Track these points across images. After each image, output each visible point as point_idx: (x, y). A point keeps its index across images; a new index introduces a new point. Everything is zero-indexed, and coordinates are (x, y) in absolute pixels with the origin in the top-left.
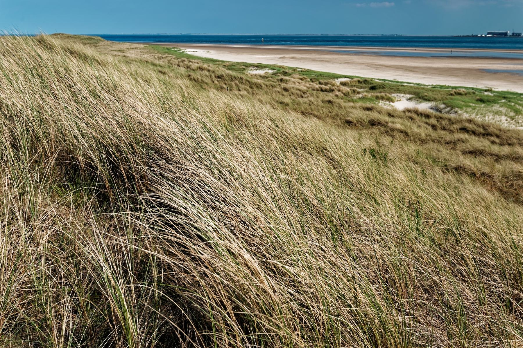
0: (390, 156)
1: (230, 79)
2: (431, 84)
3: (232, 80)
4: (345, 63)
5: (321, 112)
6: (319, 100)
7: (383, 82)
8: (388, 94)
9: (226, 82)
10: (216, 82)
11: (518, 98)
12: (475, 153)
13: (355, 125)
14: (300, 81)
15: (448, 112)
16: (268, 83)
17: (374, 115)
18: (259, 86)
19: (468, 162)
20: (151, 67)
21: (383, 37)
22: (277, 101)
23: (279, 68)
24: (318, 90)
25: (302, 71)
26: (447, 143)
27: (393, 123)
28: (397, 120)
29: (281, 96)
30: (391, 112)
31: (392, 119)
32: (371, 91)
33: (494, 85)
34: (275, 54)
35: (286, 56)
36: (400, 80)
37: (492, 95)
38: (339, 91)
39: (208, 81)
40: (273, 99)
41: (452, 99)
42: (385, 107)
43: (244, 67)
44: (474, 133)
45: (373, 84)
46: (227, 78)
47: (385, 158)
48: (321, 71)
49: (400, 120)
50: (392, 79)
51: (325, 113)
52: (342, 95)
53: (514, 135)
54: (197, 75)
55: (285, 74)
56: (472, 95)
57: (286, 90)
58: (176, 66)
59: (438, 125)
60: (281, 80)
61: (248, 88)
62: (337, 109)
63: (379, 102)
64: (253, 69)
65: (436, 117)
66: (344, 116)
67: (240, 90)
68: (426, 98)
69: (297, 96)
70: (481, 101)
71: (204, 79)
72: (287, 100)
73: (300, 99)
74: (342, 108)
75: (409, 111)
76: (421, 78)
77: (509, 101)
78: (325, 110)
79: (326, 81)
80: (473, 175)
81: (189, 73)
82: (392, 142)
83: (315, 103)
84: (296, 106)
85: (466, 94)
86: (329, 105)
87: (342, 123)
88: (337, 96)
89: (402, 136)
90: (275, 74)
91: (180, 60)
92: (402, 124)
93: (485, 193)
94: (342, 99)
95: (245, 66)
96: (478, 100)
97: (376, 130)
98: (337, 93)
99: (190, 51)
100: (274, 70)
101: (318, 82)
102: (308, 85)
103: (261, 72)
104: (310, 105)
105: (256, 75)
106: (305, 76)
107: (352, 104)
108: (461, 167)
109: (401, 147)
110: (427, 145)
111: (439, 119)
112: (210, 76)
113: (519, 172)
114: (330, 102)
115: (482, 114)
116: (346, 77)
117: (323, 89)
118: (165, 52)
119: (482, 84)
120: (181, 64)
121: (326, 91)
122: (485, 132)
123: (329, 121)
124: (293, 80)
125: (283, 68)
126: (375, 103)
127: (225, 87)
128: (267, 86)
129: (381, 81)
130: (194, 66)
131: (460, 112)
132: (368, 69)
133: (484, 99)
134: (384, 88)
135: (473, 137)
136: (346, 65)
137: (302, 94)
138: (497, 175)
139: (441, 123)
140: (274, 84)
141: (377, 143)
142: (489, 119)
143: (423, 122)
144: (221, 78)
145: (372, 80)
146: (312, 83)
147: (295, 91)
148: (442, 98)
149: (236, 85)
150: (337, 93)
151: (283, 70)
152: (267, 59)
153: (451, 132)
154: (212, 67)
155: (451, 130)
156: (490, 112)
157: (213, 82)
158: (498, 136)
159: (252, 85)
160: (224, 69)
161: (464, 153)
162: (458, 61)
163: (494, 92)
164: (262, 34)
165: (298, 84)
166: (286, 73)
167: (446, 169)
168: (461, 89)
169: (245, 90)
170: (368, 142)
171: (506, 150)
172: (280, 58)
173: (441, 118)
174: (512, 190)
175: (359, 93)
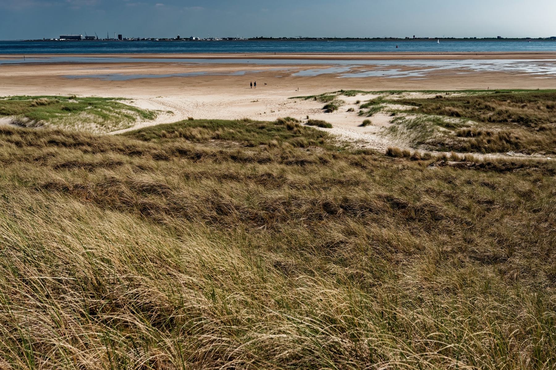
2: (7, 96)
11: (104, 103)
12: (67, 165)
15: (33, 125)
19: (59, 177)
26: (37, 160)
33: (78, 92)
37: (77, 102)
41: (34, 111)
44: (65, 144)
53: (105, 141)
56: (56, 104)
65: (18, 132)
68: (4, 112)
70: (67, 109)
77: (96, 107)
80: (65, 190)
85: (49, 104)
96: (63, 109)
108: (51, 184)
110: (13, 166)
111: (22, 134)
113: (113, 178)
115: (70, 124)
119: (65, 92)
122: (76, 142)
131: (46, 124)
133: (70, 108)
135: (64, 149)
139: (25, 139)
143: (3, 140)
148: (23, 110)
153: (39, 147)
155: (38, 145)
156: (78, 120)
158: (89, 145)
161: (56, 168)
163: (79, 99)
167: (35, 188)
168: (43, 99)
171: (99, 157)
173: (24, 133)
174: (107, 197)
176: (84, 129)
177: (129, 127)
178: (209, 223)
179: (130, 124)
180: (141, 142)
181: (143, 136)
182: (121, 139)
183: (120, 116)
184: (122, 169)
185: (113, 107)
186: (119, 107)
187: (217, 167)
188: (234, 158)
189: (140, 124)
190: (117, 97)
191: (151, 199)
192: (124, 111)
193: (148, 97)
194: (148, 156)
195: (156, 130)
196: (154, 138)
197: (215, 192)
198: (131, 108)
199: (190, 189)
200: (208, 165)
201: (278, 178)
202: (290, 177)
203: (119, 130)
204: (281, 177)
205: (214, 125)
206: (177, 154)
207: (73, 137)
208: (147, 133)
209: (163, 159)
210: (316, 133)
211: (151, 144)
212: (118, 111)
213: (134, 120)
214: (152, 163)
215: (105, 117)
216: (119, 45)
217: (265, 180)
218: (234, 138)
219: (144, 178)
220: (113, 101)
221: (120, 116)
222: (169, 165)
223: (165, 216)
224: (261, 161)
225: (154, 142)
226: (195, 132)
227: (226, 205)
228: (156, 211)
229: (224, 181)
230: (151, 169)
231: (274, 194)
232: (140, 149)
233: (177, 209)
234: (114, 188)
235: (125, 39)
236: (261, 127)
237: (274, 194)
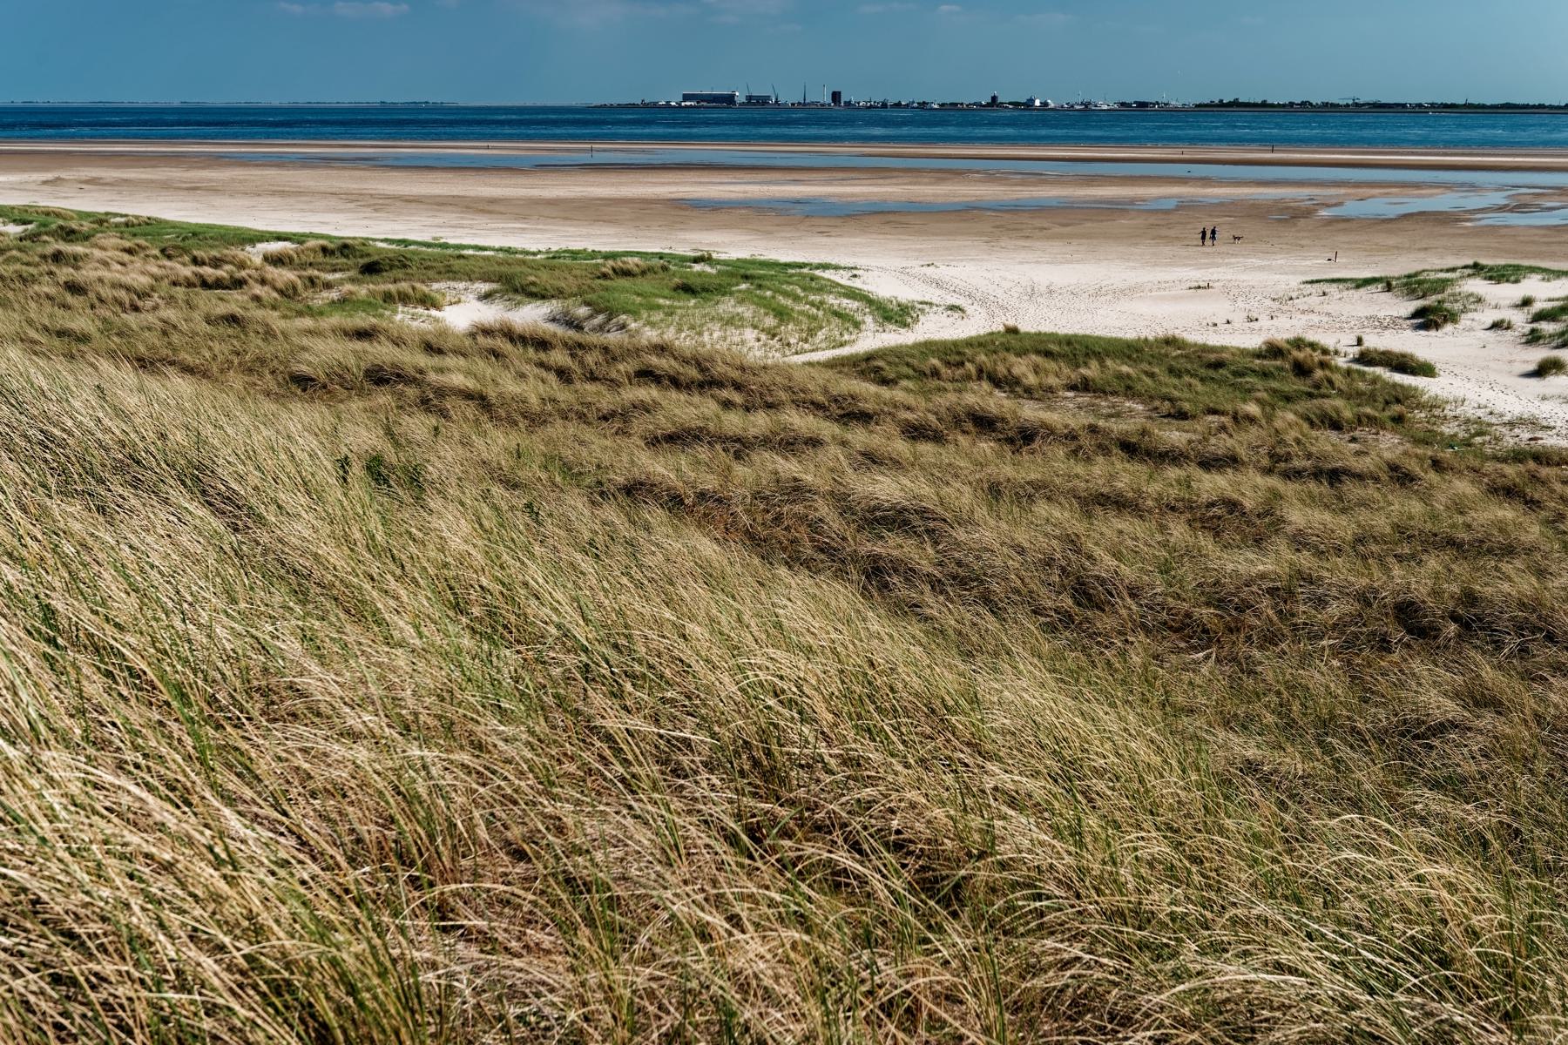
0: (432, 472)
4: (273, 193)
5: (207, 355)
6: (197, 316)
7: (401, 248)
8: (418, 285)
11: (782, 277)
12: (678, 438)
13: (325, 387)
14: (126, 257)
15: (601, 328)
17: (382, 352)
19: (660, 467)
21: (385, 108)
22: (46, 329)
23: (42, 218)
24: (190, 284)
25: (127, 225)
26: (605, 418)
27: (441, 371)
28: (450, 361)
29: (60, 312)
30: (433, 341)
31: (436, 361)
32: (367, 277)
33: (717, 244)
34: (24, 170)
36: (452, 241)
37: (714, 271)
38: (263, 282)
40: (30, 322)
42: (415, 324)
44: (676, 382)
45: (368, 255)
47: (415, 479)
48: (193, 220)
49: (462, 362)
52: (275, 295)
55: (69, 235)
56: (661, 274)
57: (74, 288)
59: (575, 366)
60: (57, 257)
62: (259, 342)
63: (395, 312)
65: (565, 344)
66: (286, 363)
68: (534, 289)
69: (119, 310)
70: (687, 289)
72: (81, 322)
73: (131, 319)
74: (275, 336)
75: (487, 332)
76: (513, 231)
77: (760, 287)
78: (217, 347)
79: (214, 253)
80: (675, 503)
82: (436, 429)
83: (184, 326)
85: (643, 273)
86: (230, 331)
87: (279, 384)
88: (257, 298)
89: (470, 410)
90: (33, 237)
92: (468, 373)
93: (707, 547)
94: (274, 308)
96: (677, 288)
97: (383, 398)
98: (258, 290)
100: (25, 223)
101: (187, 259)
102: (155, 270)
104: (165, 333)
106: (142, 242)
107: (308, 322)
108: (641, 484)
109: (465, 443)
110: (550, 429)
111: (575, 348)
113: (796, 480)
114: (232, 319)
115: (692, 328)
116: (280, 237)
117: (210, 280)
119: (683, 242)
121: (218, 284)
122: (704, 377)
123: (237, 380)
124: (97, 253)
125: (58, 215)
126: (382, 316)
129: (393, 247)
131: (633, 325)
133: (694, 285)
134: (405, 266)
135: (674, 394)
136: (277, 200)
137: (136, 299)
139: (581, 363)
140: (31, 270)
141: (389, 432)
142: (713, 339)
143: (529, 361)
145: (365, 242)
146: (168, 263)
147: (106, 292)
148: (579, 287)
150: (258, 290)
151: (61, 222)
153: (614, 384)
155: (612, 381)
156: (712, 319)
158: (738, 387)
161: (653, 442)
162: (613, 177)
163: (718, 262)
165: (119, 267)
166: (73, 232)
167: (600, 493)
168: (629, 259)
170: (363, 437)
171: (760, 422)
172: (45, 183)
173: (580, 346)
174: (778, 531)
175: (328, 286)
176: (725, 345)
177: (842, 345)
178: (1051, 628)
179: (846, 337)
180: (873, 388)
181: (878, 369)
182: (823, 376)
183: (821, 313)
184: (821, 456)
185: (804, 289)
186: (820, 290)
187: (1080, 469)
188: (1130, 449)
189: (872, 339)
190: (816, 261)
191: (893, 546)
192: (831, 300)
193: (898, 263)
194: (889, 427)
195: (913, 356)
196: (908, 377)
197: (1072, 542)
198: (852, 294)
199: (1004, 526)
200: (1054, 463)
201: (1259, 516)
202: (1297, 516)
203: (817, 350)
204: (1268, 513)
205: (1076, 350)
206: (969, 426)
207: (698, 364)
208: (889, 363)
209: (927, 438)
210: (1380, 392)
211: (898, 394)
212: (817, 298)
213: (857, 325)
214: (901, 447)
215: (782, 315)
216: (833, 120)
217: (1218, 519)
218: (1130, 391)
219: (878, 486)
220: (805, 271)
221: (821, 313)
222: (947, 455)
223: (929, 598)
224: (1210, 463)
225: (907, 390)
226: (1022, 367)
227: (1102, 581)
228: (907, 579)
229: (1098, 510)
230: (897, 464)
231: (1242, 563)
232: (869, 407)
233: (964, 580)
234: (799, 508)
235: (848, 104)
236: (1213, 363)
237: (1242, 563)
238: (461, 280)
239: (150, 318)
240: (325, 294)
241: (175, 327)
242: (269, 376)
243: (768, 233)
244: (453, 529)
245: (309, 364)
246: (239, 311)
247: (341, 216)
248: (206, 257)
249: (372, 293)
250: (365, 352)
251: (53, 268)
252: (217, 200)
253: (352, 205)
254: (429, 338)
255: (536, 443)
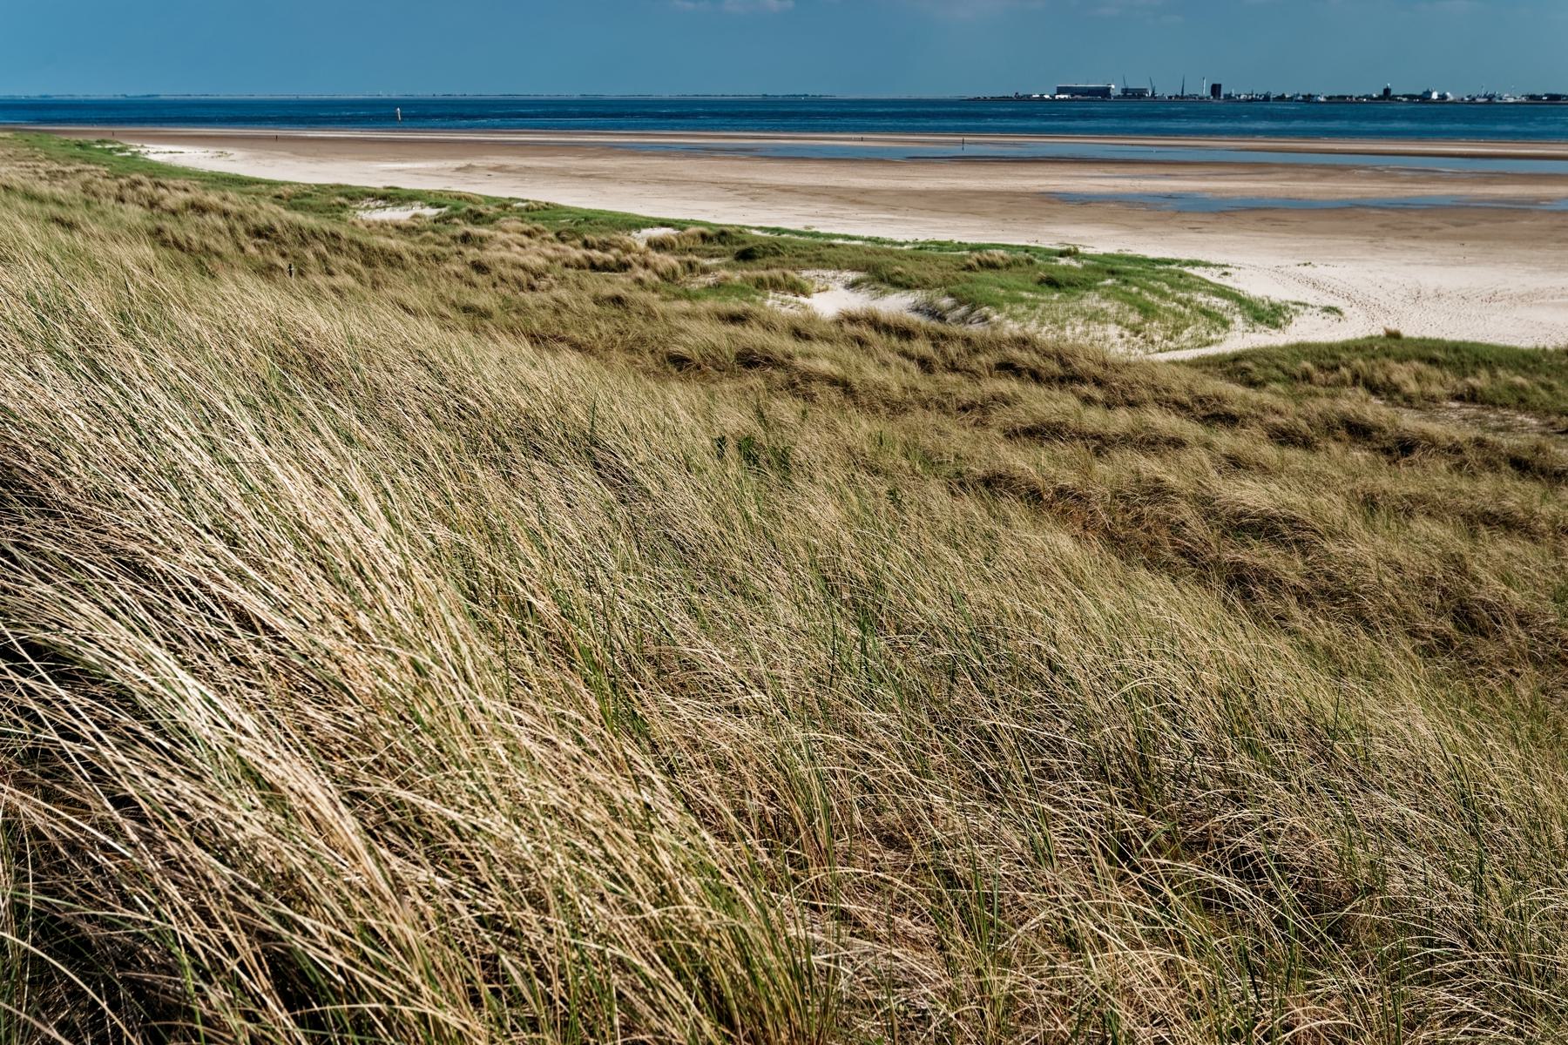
0: (799, 454)
1: (296, 241)
2: (910, 239)
3: (304, 243)
4: (661, 182)
5: (594, 333)
7: (775, 236)
8: (789, 272)
9: (285, 249)
10: (251, 250)
12: (1039, 433)
13: (699, 367)
14: (525, 240)
15: (963, 319)
16: (424, 249)
17: (753, 336)
18: (393, 260)
19: (1021, 460)
20: (22, 205)
21: (766, 101)
22: (454, 304)
24: (580, 266)
25: (527, 209)
26: (965, 409)
27: (808, 356)
28: (818, 347)
29: (467, 289)
31: (803, 346)
32: (742, 264)
33: (1082, 238)
34: (440, 158)
35: (475, 162)
37: (1079, 266)
38: (646, 266)
39: (226, 247)
40: (441, 297)
41: (971, 281)
42: (784, 310)
43: (342, 200)
44: (1036, 376)
45: (744, 242)
46: (288, 237)
47: (783, 461)
48: (586, 206)
49: (827, 347)
50: (799, 226)
51: (605, 336)
52: (656, 278)
53: (1141, 377)
54: (187, 229)
55: (476, 218)
56: (1026, 267)
57: (479, 267)
58: (112, 201)
59: (937, 357)
60: (466, 238)
61: (359, 266)
62: (641, 322)
63: (766, 297)
64: (372, 205)
65: (929, 335)
66: (663, 343)
67: (331, 273)
68: (899, 279)
70: (1052, 283)
71: (211, 242)
72: (484, 300)
73: (527, 297)
74: (655, 317)
75: (853, 320)
76: (883, 221)
77: (1126, 282)
78: (603, 326)
79: (603, 237)
81: (158, 223)
82: (804, 413)
83: (574, 306)
84: (514, 315)
85: (1008, 266)
86: (615, 312)
88: (640, 281)
89: (835, 395)
90: (445, 219)
91: (124, 181)
92: (833, 360)
93: (1065, 543)
94: (655, 291)
95: (346, 196)
96: (1041, 282)
97: (755, 380)
98: (641, 273)
99: (158, 152)
100: (439, 206)
101: (578, 242)
102: (550, 252)
103: (401, 215)
104: (557, 312)
105: (383, 225)
106: (539, 225)
107: (685, 305)
108: (1001, 476)
109: (832, 428)
110: (909, 418)
111: (937, 339)
112: (232, 230)
113: (1157, 480)
114: (617, 300)
115: (1055, 321)
116: (663, 224)
117: (598, 263)
118: (74, 157)
119: (1050, 236)
120: (128, 193)
121: (606, 267)
123: (619, 359)
124: (501, 235)
125: (468, 199)
126: (754, 301)
127: (281, 263)
128: (418, 257)
130: (174, 199)
131: (995, 318)
132: (727, 199)
133: (1058, 279)
134: (778, 254)
135: (1034, 388)
136: (663, 188)
137: (532, 279)
138: (1099, 491)
139: (943, 353)
140: (443, 249)
141: (760, 414)
142: (1075, 334)
143: (892, 350)
144: (267, 237)
145: (742, 229)
146: (561, 246)
147: (507, 272)
149: (318, 255)
150: (641, 273)
151: (470, 206)
152: (417, 173)
153: (974, 375)
154: (235, 201)
155: (972, 372)
156: (1076, 314)
157: (242, 250)
158: (1099, 383)
159: (369, 256)
160: (276, 208)
161: (1011, 435)
162: (983, 170)
163: (1085, 256)
164: (395, 94)
166: (480, 215)
167: (959, 483)
169: (348, 271)
170: (735, 419)
171: (1122, 420)
172: (458, 169)
173: (943, 336)
174: (1139, 532)
175: (705, 271)
176: (1088, 340)
177: (1208, 344)
178: (1428, 652)
179: (1213, 336)
180: (1240, 390)
181: (1246, 371)
182: (1187, 375)
183: (1188, 311)
184: (1186, 457)
185: (1172, 286)
186: (1189, 287)
187: (1464, 485)
188: (1521, 465)
189: (1240, 339)
190: (1185, 257)
191: (1258, 554)
192: (1200, 298)
193: (1271, 261)
194: (1257, 431)
195: (1284, 359)
196: (1277, 380)
198: (1222, 292)
199: (1380, 541)
200: (1434, 477)
203: (1182, 348)
206: (1342, 433)
207: (1060, 359)
208: (1258, 365)
209: (1294, 444)
211: (1266, 397)
212: (1186, 296)
213: (1225, 324)
215: (1147, 311)
216: (1214, 113)
219: (1247, 492)
220: (1174, 267)
221: (1188, 311)
222: (1318, 462)
223: (1295, 611)
225: (1275, 393)
226: (1402, 374)
227: (1488, 606)
228: (1271, 590)
229: (1484, 531)
230: (1265, 470)
232: (1235, 409)
233: (1335, 595)
234: (1160, 510)
235: (1228, 97)
238: (829, 268)
239: (545, 297)
240: (702, 279)
241: (566, 306)
242: (648, 356)
243: (1135, 229)
244: (821, 511)
245: (685, 344)
246: (622, 292)
247: (721, 204)
248: (594, 240)
249: (745, 279)
250: (738, 336)
251: (462, 249)
252: (611, 188)
253: (730, 194)
254: (799, 324)
255: (895, 431)
